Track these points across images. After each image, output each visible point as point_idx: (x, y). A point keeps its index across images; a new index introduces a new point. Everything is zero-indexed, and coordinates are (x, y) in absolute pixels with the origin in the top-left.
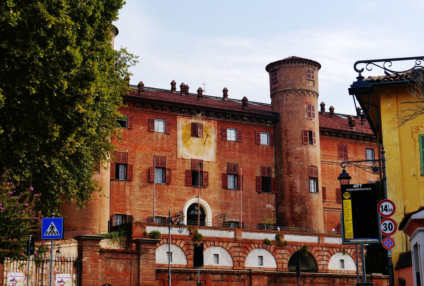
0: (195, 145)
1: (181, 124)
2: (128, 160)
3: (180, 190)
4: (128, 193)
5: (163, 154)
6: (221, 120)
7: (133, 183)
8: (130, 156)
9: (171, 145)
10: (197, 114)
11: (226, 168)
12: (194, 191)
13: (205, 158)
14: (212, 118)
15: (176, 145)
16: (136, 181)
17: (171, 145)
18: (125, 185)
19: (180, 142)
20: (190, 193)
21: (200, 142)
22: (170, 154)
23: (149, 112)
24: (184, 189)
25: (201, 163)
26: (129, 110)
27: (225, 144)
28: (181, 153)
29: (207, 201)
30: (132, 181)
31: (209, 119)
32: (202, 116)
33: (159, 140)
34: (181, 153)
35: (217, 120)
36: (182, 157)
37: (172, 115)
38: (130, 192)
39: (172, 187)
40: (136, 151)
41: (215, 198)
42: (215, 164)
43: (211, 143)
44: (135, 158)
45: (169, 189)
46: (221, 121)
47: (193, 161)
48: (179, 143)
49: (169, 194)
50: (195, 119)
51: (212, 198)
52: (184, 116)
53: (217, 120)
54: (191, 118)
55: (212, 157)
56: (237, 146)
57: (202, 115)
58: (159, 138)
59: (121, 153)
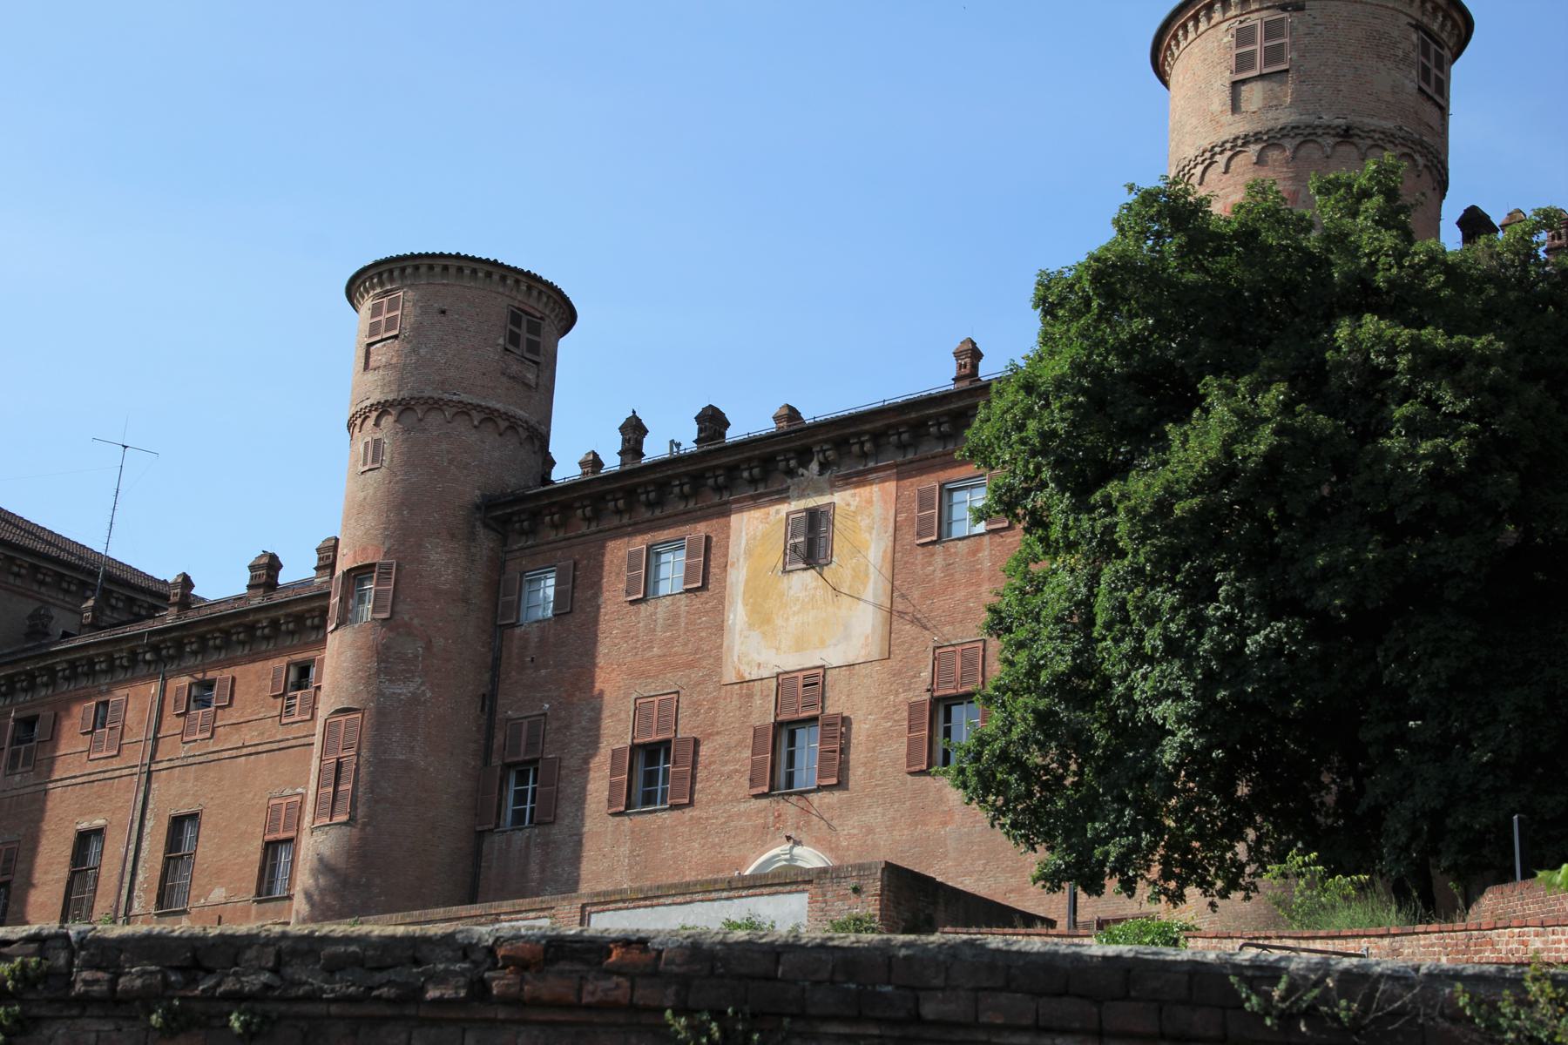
0: (798, 607)
1: (744, 533)
2: (547, 740)
3: (725, 823)
4: (536, 876)
5: (670, 681)
6: (910, 456)
7: (555, 830)
8: (555, 724)
9: (703, 634)
10: (801, 471)
11: (926, 674)
12: (779, 815)
13: (833, 656)
14: (871, 465)
15: (720, 628)
16: (567, 821)
17: (703, 634)
18: (527, 846)
19: (737, 615)
20: (765, 826)
21: (816, 588)
22: (696, 675)
23: (630, 525)
24: (740, 815)
25: (815, 681)
26: (564, 543)
27: (930, 564)
28: (736, 659)
29: (831, 850)
30: (553, 823)
31: (858, 474)
32: (821, 473)
33: (658, 629)
34: (736, 659)
35: (896, 466)
36: (742, 676)
37: (711, 511)
38: (543, 870)
39: (692, 818)
40: (575, 699)
41: (870, 830)
42: (877, 667)
43: (867, 575)
44: (568, 727)
45: (681, 829)
46: (911, 462)
47: (783, 680)
48: (732, 617)
49: (680, 848)
50: (801, 497)
51: (855, 831)
52: (755, 498)
53: (896, 466)
54: (782, 496)
55: (867, 637)
56: (984, 554)
57: (824, 467)
58: (660, 621)
59: (525, 722)
